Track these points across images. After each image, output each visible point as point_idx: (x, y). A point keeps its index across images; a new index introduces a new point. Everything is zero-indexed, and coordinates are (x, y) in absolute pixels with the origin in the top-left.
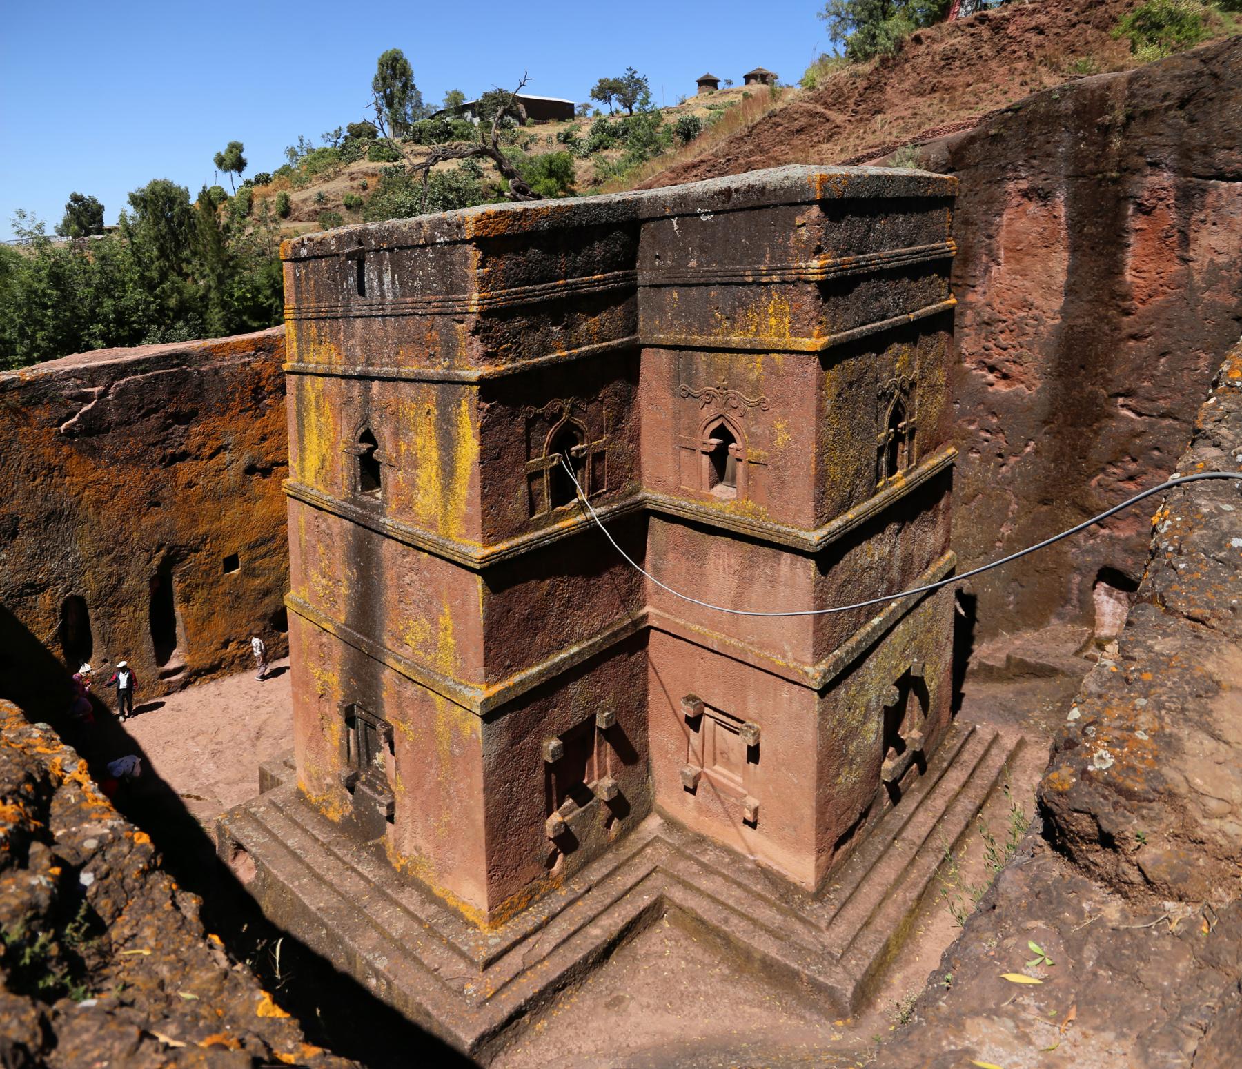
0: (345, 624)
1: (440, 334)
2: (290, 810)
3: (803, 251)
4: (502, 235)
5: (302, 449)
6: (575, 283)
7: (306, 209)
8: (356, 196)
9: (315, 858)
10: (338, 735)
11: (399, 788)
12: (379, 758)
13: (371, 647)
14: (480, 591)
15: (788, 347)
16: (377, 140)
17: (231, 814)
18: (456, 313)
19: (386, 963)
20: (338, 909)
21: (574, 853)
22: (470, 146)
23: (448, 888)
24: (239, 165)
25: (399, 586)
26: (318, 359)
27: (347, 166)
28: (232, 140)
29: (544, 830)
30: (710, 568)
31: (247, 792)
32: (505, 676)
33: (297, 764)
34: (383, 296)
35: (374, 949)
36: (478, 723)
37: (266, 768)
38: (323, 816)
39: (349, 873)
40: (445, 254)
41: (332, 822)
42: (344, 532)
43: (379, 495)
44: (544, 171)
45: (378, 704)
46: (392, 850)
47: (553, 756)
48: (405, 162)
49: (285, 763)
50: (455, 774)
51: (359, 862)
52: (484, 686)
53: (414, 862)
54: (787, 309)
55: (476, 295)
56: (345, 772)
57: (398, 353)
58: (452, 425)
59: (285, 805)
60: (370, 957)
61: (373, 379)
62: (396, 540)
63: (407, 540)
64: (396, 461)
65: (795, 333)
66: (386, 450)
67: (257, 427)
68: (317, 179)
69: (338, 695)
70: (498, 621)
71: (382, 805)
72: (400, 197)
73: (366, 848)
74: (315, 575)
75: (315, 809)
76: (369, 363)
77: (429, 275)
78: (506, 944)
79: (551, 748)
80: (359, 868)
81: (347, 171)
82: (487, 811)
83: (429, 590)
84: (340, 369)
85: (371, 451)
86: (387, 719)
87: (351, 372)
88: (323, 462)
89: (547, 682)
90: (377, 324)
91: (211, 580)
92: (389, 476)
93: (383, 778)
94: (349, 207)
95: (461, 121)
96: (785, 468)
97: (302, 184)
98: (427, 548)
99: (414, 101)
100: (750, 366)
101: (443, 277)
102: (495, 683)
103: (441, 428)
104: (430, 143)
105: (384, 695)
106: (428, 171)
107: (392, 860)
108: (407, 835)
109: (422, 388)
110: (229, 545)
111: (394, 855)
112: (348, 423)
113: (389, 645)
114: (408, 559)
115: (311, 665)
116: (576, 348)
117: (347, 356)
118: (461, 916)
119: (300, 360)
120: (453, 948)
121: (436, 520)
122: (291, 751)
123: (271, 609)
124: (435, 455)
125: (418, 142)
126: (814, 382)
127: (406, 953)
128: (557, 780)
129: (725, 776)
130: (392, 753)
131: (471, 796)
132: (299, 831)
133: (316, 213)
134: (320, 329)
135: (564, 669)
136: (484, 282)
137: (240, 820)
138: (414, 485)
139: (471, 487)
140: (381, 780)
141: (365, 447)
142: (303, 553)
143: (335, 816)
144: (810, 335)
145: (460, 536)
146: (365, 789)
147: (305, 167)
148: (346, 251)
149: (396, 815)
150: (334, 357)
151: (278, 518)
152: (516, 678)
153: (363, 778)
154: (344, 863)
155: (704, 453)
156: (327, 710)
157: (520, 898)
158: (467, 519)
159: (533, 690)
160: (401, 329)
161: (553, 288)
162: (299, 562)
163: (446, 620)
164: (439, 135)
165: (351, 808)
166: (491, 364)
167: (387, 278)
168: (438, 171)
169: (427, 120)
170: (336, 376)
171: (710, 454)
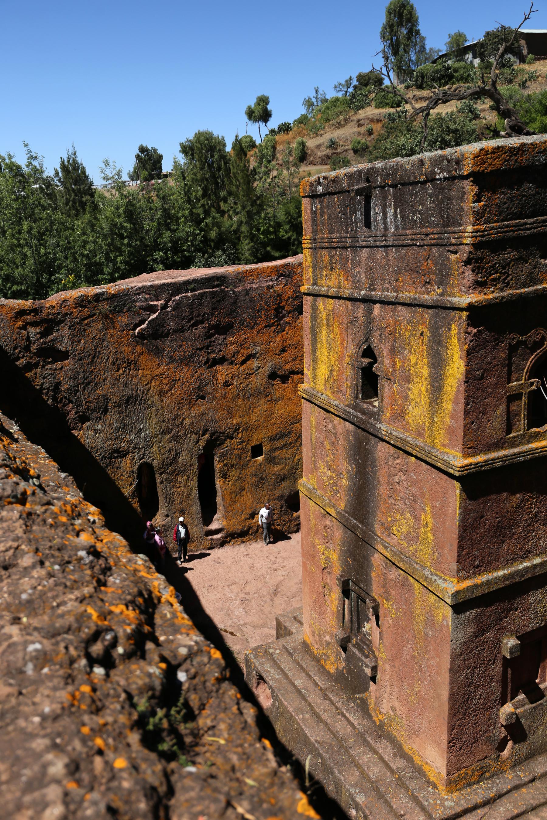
0: (345, 511)
1: (436, 264)
2: (299, 657)
4: (498, 170)
7: (320, 154)
8: (363, 141)
9: (314, 698)
10: (336, 603)
11: (382, 655)
12: (367, 627)
13: (365, 532)
14: (458, 496)
16: (383, 86)
17: (255, 650)
18: (451, 245)
19: (364, 799)
20: (331, 745)
21: (522, 744)
22: (469, 88)
23: (416, 748)
25: (389, 484)
27: (356, 113)
29: (497, 716)
31: (268, 636)
32: (474, 575)
33: (304, 620)
34: (386, 228)
35: (355, 785)
36: (449, 611)
37: (281, 619)
38: (322, 666)
39: (340, 717)
40: (443, 189)
41: (329, 672)
42: (346, 433)
43: (376, 404)
45: (368, 582)
46: (373, 706)
47: (511, 653)
48: (408, 107)
49: (295, 618)
50: (427, 652)
51: (348, 710)
52: (455, 580)
53: (390, 719)
55: (470, 228)
56: (341, 634)
57: (397, 280)
58: (442, 346)
59: (295, 652)
60: (352, 790)
61: (375, 302)
62: (389, 443)
63: (398, 444)
64: (392, 375)
68: (330, 127)
69: (337, 570)
70: (472, 525)
71: (367, 666)
73: (353, 699)
74: (322, 467)
75: (317, 660)
76: (372, 288)
77: (428, 209)
78: (459, 809)
79: (510, 645)
80: (348, 715)
81: (355, 118)
82: (451, 689)
83: (415, 490)
84: (347, 293)
85: (371, 365)
86: (374, 595)
87: (356, 296)
89: (510, 586)
90: (380, 254)
93: (369, 644)
94: (356, 151)
95: (462, 63)
97: (317, 132)
98: (414, 453)
101: (441, 210)
102: (465, 579)
103: (432, 348)
104: (432, 87)
105: (373, 574)
106: (428, 114)
107: (373, 714)
108: (386, 695)
109: (417, 312)
111: (375, 710)
112: (353, 340)
113: (379, 533)
114: (398, 461)
117: (353, 281)
118: (424, 774)
119: (315, 284)
120: (416, 800)
121: (424, 429)
122: (300, 609)
124: (425, 372)
125: (420, 87)
127: (380, 796)
128: (512, 674)
130: (378, 624)
131: (439, 673)
132: (303, 675)
133: (328, 157)
135: (527, 577)
136: (478, 216)
137: (262, 657)
139: (455, 403)
140: (368, 646)
141: (366, 361)
142: (314, 448)
143: (332, 669)
145: (444, 445)
146: (355, 650)
147: (319, 116)
148: (356, 187)
149: (378, 677)
152: (483, 578)
153: (354, 641)
154: (337, 708)
156: (328, 581)
157: (473, 772)
158: (451, 431)
159: (496, 590)
160: (401, 259)
162: (310, 454)
163: (427, 518)
164: (440, 79)
165: (343, 664)
166: (480, 292)
167: (390, 212)
168: (438, 114)
169: (429, 65)
170: (344, 298)
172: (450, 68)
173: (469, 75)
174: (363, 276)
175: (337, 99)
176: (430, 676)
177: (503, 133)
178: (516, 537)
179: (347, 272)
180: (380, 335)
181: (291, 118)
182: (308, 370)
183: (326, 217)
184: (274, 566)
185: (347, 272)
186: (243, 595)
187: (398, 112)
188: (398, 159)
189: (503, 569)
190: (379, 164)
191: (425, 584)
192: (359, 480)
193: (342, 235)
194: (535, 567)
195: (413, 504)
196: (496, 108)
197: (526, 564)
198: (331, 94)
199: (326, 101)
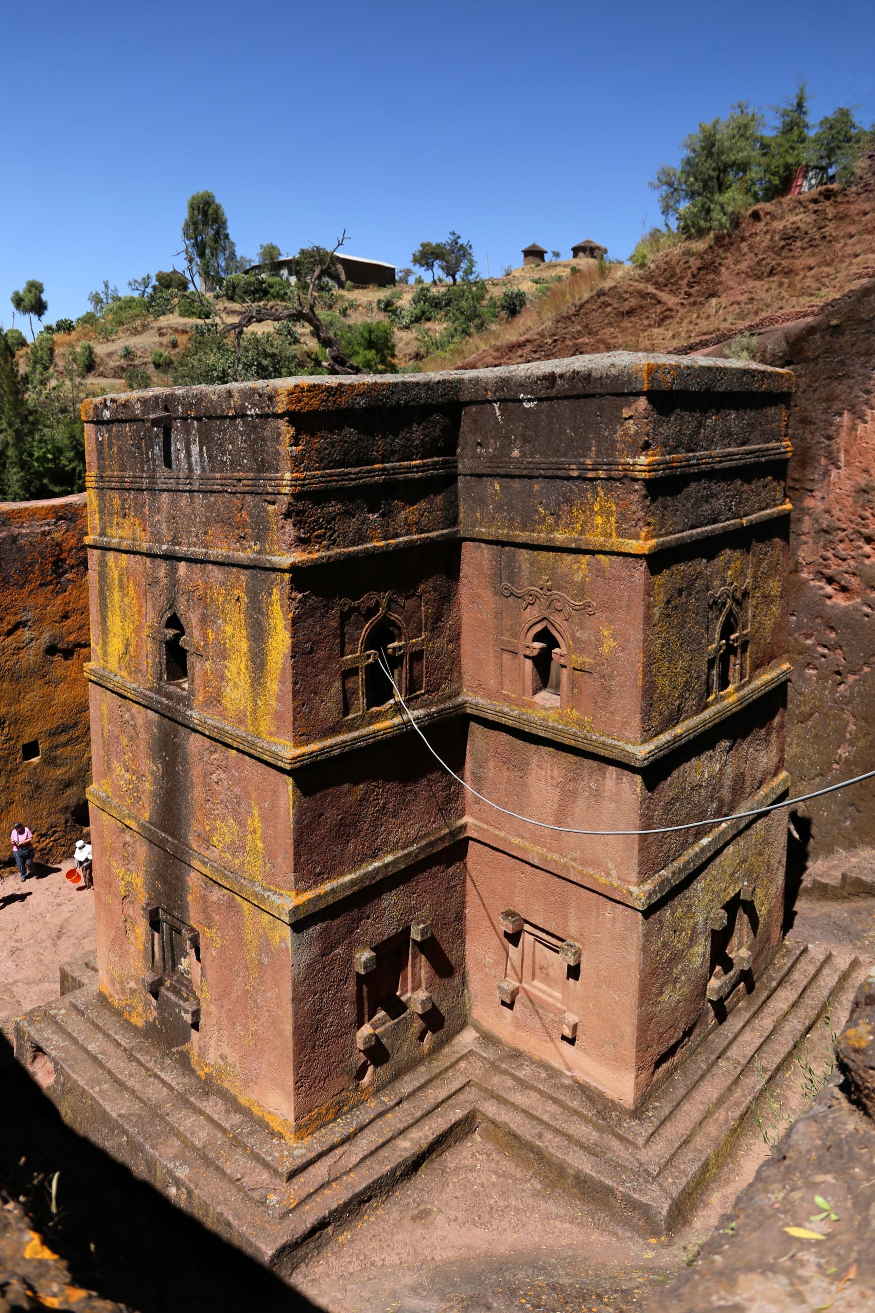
0: (149, 822)
3: (630, 446)
5: (105, 631)
6: (393, 468)
7: (112, 364)
8: (166, 354)
10: (143, 939)
11: (205, 995)
12: (184, 964)
13: (176, 847)
15: (615, 549)
16: (187, 293)
22: (286, 308)
23: (254, 1097)
24: (39, 308)
25: (205, 784)
26: (121, 534)
27: (156, 319)
28: (31, 278)
32: (316, 884)
33: (99, 967)
34: (190, 469)
36: (288, 930)
37: (68, 969)
38: (126, 1021)
41: (135, 1027)
42: (148, 723)
43: (186, 686)
44: (362, 341)
45: (183, 908)
46: (196, 1058)
48: (218, 320)
49: (87, 965)
50: (262, 983)
51: (162, 1069)
52: (294, 893)
53: (219, 1071)
54: (614, 508)
56: (149, 977)
61: (180, 559)
62: (203, 734)
63: (214, 735)
64: (204, 650)
65: (622, 533)
66: (193, 638)
67: (57, 604)
68: (124, 331)
69: (142, 898)
70: (309, 826)
71: (186, 1012)
72: (212, 359)
73: (169, 1055)
75: (119, 1014)
76: (175, 542)
78: (311, 1155)
80: (163, 1075)
81: (156, 325)
82: (295, 1021)
83: (237, 790)
84: (145, 547)
85: (177, 637)
86: (192, 923)
88: (127, 646)
89: (359, 891)
91: (9, 767)
92: (195, 665)
93: (188, 984)
94: (157, 366)
95: (277, 279)
97: (107, 336)
98: (235, 745)
99: (227, 253)
100: (575, 567)
102: (305, 890)
104: (244, 301)
105: (190, 898)
106: (241, 332)
107: (197, 1068)
108: (213, 1043)
110: (29, 730)
111: (199, 1063)
112: (153, 606)
113: (194, 846)
114: (215, 756)
115: (115, 864)
116: (393, 538)
117: (152, 533)
118: (267, 1126)
119: (103, 534)
120: (257, 1158)
122: (94, 952)
123: (73, 802)
125: (231, 299)
126: (642, 587)
130: (198, 959)
131: (279, 1006)
133: (123, 369)
135: (378, 878)
138: (222, 677)
140: (187, 987)
141: (171, 633)
142: (106, 744)
143: (138, 1021)
144: (637, 537)
146: (170, 994)
147: (110, 317)
149: (201, 1022)
150: (139, 533)
151: (81, 703)
152: (327, 887)
153: (168, 984)
156: (131, 912)
159: (343, 899)
161: (369, 472)
162: (102, 753)
163: (254, 822)
164: (254, 293)
165: (155, 1014)
167: (195, 449)
168: (253, 333)
169: (240, 275)
170: (141, 554)
171: (533, 659)
172: (264, 282)
173: (286, 294)
174: (164, 526)
175: (132, 300)
176: (268, 1011)
177: (325, 364)
178: (362, 834)
179: (144, 520)
180: (188, 601)
181: (74, 315)
182: (97, 644)
183: (115, 449)
184: (58, 901)
185: (144, 520)
186: (13, 944)
187: (207, 325)
188: (203, 387)
189: (350, 873)
190: (179, 391)
191: (256, 902)
192: (167, 782)
193: (137, 474)
194: (386, 866)
195: (237, 806)
196: (316, 333)
197: (377, 864)
198: (125, 292)
199: (119, 299)
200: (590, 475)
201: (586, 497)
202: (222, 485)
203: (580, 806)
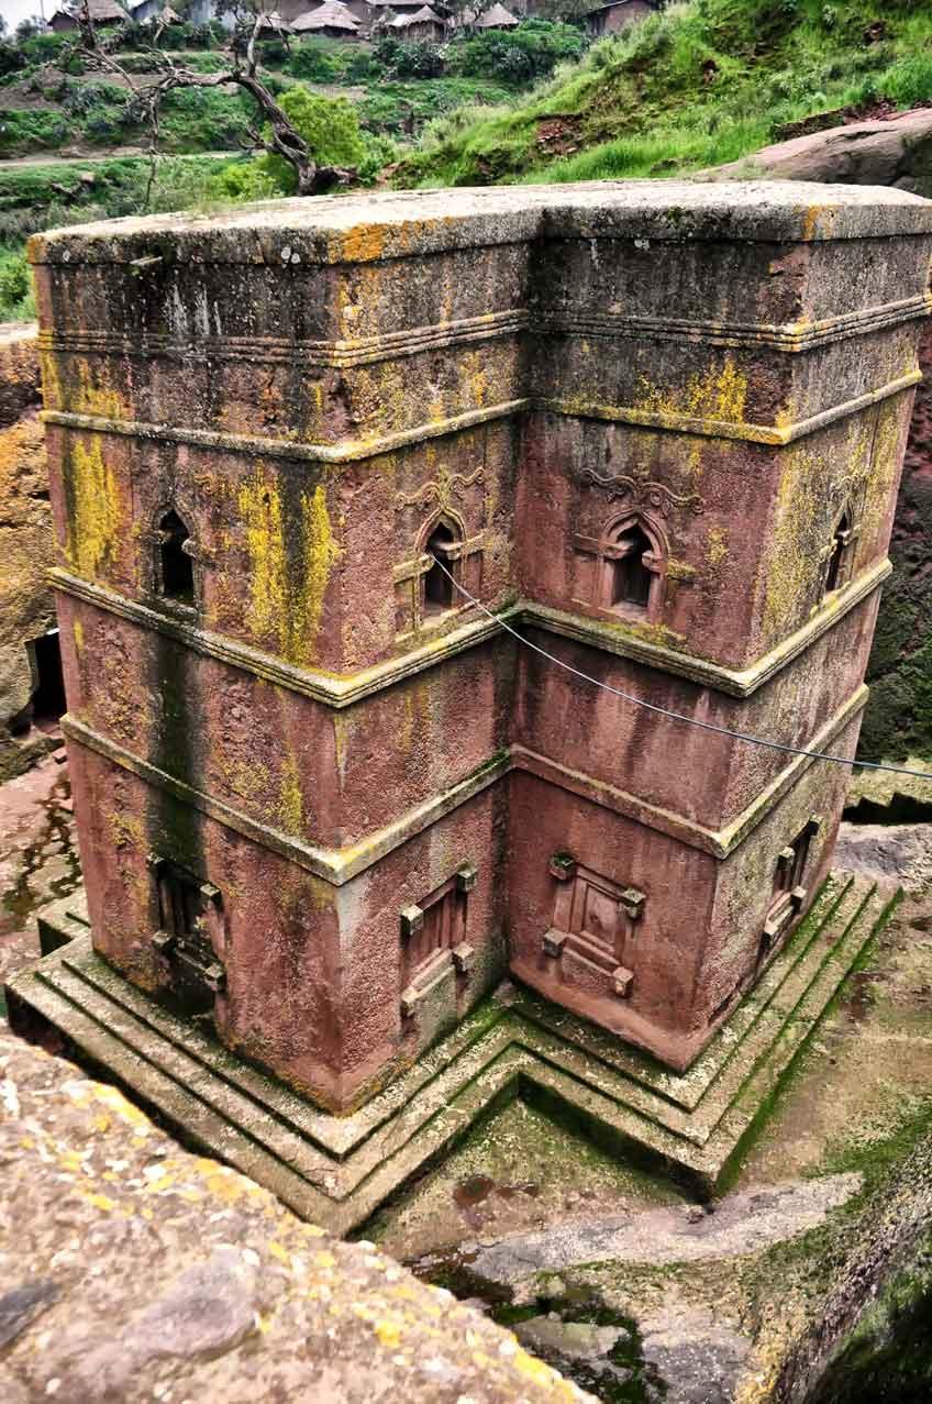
30: (601, 703)
66: (201, 540)
88: (107, 551)
96: (716, 590)
114: (234, 687)
117: (138, 410)
129: (593, 944)
134: (94, 368)
138: (244, 593)
155: (607, 559)
174: (156, 401)
176: (310, 980)
185: (126, 394)
200: (718, 342)
201: (709, 371)
202: (241, 352)
203: (659, 739)
